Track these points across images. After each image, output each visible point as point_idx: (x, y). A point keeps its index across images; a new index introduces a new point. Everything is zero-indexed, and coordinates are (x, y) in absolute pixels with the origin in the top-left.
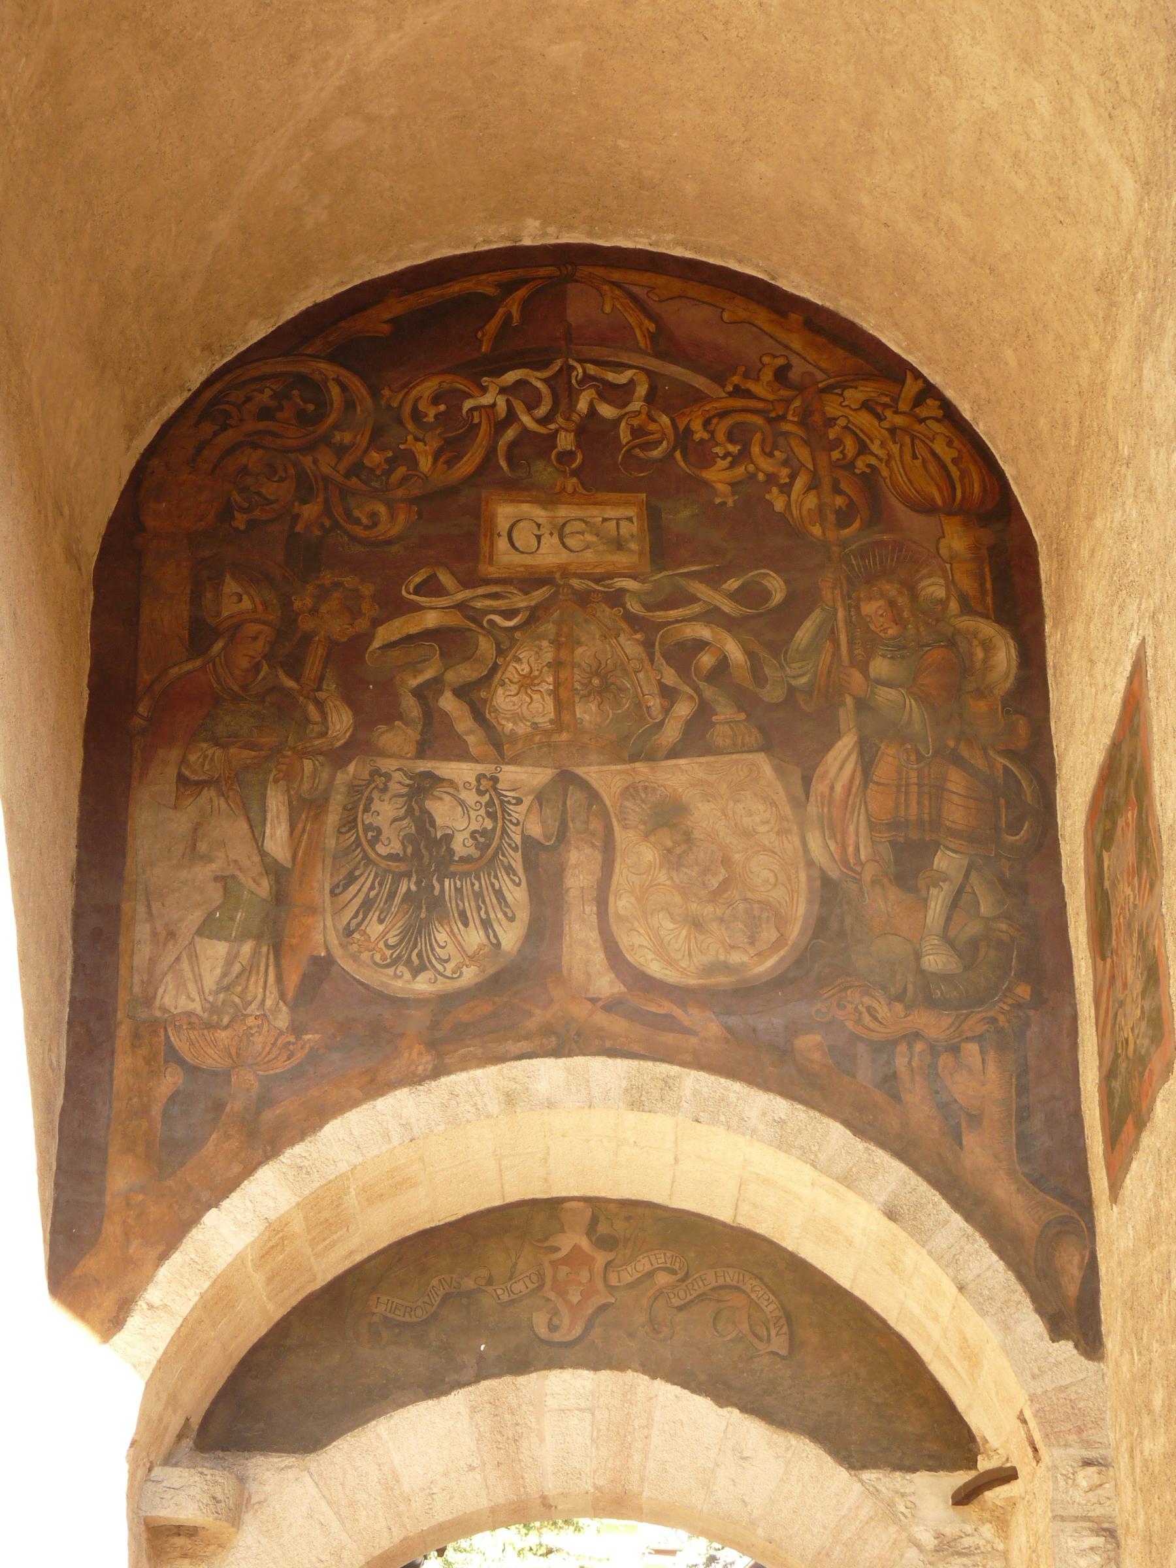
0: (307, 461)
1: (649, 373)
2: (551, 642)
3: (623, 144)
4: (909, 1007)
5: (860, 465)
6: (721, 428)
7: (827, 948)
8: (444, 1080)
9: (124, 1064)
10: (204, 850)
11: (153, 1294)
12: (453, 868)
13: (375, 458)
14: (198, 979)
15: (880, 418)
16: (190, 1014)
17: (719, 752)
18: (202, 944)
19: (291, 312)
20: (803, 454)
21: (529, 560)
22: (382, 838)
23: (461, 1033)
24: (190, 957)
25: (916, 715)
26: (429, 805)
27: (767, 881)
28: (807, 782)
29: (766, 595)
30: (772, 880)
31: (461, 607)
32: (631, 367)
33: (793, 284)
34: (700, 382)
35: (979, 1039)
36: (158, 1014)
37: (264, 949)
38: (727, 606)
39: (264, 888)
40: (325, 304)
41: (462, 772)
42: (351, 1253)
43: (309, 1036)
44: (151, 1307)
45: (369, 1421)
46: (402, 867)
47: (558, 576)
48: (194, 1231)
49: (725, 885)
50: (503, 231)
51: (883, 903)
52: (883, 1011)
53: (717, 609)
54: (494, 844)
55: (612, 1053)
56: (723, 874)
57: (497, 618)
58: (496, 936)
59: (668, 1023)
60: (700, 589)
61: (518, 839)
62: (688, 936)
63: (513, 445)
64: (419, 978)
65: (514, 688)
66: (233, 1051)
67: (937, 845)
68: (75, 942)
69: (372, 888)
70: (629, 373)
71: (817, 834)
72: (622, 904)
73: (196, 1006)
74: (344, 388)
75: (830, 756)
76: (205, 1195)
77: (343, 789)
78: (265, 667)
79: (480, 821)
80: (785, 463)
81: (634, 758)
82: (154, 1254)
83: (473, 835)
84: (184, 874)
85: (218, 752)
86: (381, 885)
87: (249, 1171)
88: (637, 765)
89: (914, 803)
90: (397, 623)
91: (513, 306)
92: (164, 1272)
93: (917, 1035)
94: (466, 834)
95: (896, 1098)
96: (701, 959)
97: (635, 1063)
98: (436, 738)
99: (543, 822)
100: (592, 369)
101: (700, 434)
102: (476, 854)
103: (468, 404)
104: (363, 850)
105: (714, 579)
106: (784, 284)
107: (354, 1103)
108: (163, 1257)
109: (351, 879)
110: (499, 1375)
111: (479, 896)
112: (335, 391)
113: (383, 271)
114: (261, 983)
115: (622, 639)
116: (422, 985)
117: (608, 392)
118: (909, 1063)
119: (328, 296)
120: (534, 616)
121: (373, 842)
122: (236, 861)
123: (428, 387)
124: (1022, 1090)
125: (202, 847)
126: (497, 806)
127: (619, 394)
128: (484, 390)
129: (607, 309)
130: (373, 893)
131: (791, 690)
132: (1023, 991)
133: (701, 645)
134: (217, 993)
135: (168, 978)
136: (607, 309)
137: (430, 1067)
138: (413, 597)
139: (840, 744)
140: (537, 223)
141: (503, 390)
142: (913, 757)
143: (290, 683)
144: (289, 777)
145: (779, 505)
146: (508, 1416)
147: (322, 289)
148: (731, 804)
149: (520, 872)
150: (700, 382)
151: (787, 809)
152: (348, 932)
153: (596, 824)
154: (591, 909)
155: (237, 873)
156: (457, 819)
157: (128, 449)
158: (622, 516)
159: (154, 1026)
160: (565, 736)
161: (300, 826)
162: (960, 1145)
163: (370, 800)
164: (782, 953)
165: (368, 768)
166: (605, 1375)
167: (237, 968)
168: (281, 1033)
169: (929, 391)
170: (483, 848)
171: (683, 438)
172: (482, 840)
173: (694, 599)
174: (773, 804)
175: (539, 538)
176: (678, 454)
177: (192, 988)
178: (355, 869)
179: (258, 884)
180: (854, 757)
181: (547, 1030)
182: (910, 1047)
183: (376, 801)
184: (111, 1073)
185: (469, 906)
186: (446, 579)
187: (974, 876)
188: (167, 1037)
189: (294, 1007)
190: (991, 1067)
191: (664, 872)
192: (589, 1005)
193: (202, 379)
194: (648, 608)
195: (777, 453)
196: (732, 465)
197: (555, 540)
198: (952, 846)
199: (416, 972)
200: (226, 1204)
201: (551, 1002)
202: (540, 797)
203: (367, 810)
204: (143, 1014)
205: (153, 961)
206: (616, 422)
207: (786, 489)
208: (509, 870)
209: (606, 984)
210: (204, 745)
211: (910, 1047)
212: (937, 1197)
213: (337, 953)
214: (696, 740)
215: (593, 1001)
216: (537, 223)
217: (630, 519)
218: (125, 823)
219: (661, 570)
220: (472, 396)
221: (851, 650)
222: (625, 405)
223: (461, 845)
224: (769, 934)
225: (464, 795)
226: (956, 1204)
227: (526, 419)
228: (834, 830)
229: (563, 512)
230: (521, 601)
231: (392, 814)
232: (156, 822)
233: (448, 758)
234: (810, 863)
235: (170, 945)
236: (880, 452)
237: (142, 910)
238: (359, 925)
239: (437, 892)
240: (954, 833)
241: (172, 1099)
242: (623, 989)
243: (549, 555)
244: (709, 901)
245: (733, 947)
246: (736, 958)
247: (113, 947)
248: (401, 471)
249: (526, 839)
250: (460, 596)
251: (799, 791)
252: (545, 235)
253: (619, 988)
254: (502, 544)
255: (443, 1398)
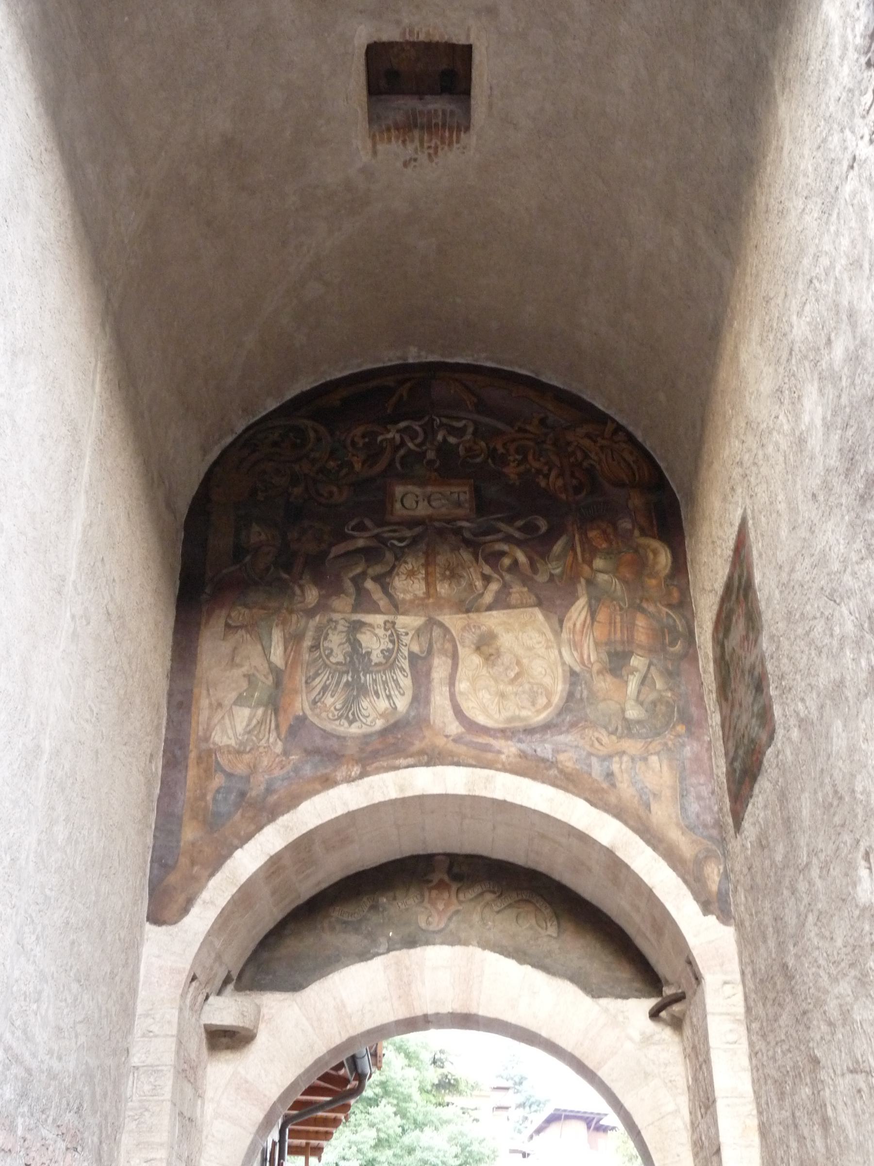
0: (297, 468)
1: (475, 423)
2: (424, 553)
3: (458, 300)
4: (620, 738)
5: (585, 464)
6: (512, 447)
7: (574, 709)
8: (366, 779)
9: (192, 773)
10: (239, 662)
11: (205, 895)
12: (371, 669)
13: (332, 464)
14: (234, 727)
15: (595, 442)
16: (228, 746)
17: (514, 607)
18: (236, 709)
19: (289, 395)
20: (555, 459)
21: (411, 513)
22: (334, 654)
23: (375, 755)
24: (229, 716)
25: (619, 587)
26: (360, 637)
27: (541, 673)
28: (561, 622)
29: (538, 528)
30: (544, 672)
31: (376, 537)
32: (465, 419)
33: (550, 378)
34: (500, 426)
35: (658, 753)
36: (212, 746)
37: (269, 712)
38: (517, 534)
39: (270, 681)
40: (308, 391)
41: (378, 619)
42: (319, 883)
43: (293, 757)
44: (204, 902)
45: (329, 974)
46: (344, 669)
47: (427, 521)
48: (229, 861)
49: (518, 675)
50: (399, 354)
51: (604, 684)
52: (605, 739)
53: (512, 537)
54: (393, 656)
55: (458, 764)
56: (517, 669)
57: (396, 543)
58: (394, 703)
59: (486, 748)
60: (502, 526)
61: (406, 654)
62: (498, 703)
63: (403, 457)
64: (353, 725)
65: (404, 577)
66: (252, 765)
67: (631, 653)
68: (168, 709)
69: (328, 679)
70: (464, 422)
71: (567, 648)
72: (462, 686)
73: (232, 742)
74: (316, 431)
75: (573, 609)
76: (236, 842)
77: (312, 629)
78: (272, 568)
79: (386, 644)
80: (546, 464)
81: (468, 611)
82: (207, 874)
83: (382, 651)
84: (228, 674)
85: (247, 611)
86: (332, 677)
87: (259, 829)
88: (471, 615)
89: (619, 632)
90: (343, 545)
91: (404, 391)
92: (212, 883)
93: (624, 752)
94: (379, 651)
95: (613, 785)
96: (506, 714)
97: (470, 769)
98: (363, 603)
99: (420, 644)
100: (444, 420)
101: (501, 450)
102: (384, 661)
103: (380, 438)
104: (323, 660)
105: (510, 521)
106: (544, 379)
107: (317, 792)
108: (212, 875)
109: (317, 674)
110: (400, 949)
111: (385, 683)
112: (312, 434)
113: (339, 375)
114: (267, 730)
115: (461, 551)
116: (355, 729)
117: (452, 430)
118: (620, 767)
119: (308, 388)
120: (415, 541)
121: (328, 657)
122: (255, 667)
123: (359, 431)
124: (682, 779)
125: (238, 660)
126: (395, 638)
127: (460, 432)
128: (388, 431)
129: (452, 392)
130: (328, 682)
131: (552, 575)
132: (681, 729)
133: (503, 554)
134: (244, 735)
135: (218, 728)
136: (452, 392)
137: (358, 772)
138: (351, 532)
139: (577, 603)
140: (416, 350)
141: (398, 431)
142: (618, 608)
143: (286, 576)
144: (284, 623)
145: (543, 484)
146: (405, 971)
147: (305, 384)
148: (521, 634)
149: (408, 670)
150: (500, 426)
151: (550, 635)
152: (315, 702)
153: (448, 646)
154: (446, 689)
155: (256, 673)
156: (374, 643)
157: (203, 460)
158: (462, 492)
159: (210, 752)
160: (431, 600)
161: (290, 648)
162: (650, 811)
163: (327, 634)
164: (549, 710)
165: (326, 618)
166: (458, 949)
167: (254, 722)
168: (278, 756)
169: (619, 428)
170: (387, 658)
171: (492, 453)
172: (387, 654)
173: (499, 531)
174: (544, 634)
175: (417, 502)
176: (490, 461)
177: (230, 732)
178: (319, 669)
179: (267, 678)
180: (586, 609)
181: (422, 752)
182: (621, 757)
183: (331, 635)
184: (185, 777)
185: (380, 688)
186: (368, 523)
187: (652, 668)
188: (216, 758)
189: (285, 741)
190: (665, 768)
191: (485, 668)
192: (445, 739)
193: (243, 427)
194: (475, 535)
195: (541, 459)
196: (518, 465)
197: (426, 503)
198: (640, 653)
199: (351, 723)
200: (246, 846)
201: (424, 737)
202: (419, 632)
203: (325, 639)
204: (204, 746)
205: (209, 718)
206: (458, 445)
207: (547, 476)
208: (402, 669)
209: (454, 728)
210: (239, 608)
211: (621, 757)
212: (637, 838)
213: (308, 712)
214: (501, 602)
215: (447, 736)
216: (416, 350)
217: (465, 493)
218: (197, 647)
219: (483, 516)
220: (382, 434)
221: (583, 556)
222: (462, 437)
223: (376, 657)
224: (542, 701)
225: (377, 631)
226: (648, 842)
227: (411, 445)
228: (575, 645)
229: (429, 489)
230: (408, 533)
231: (338, 642)
232: (212, 646)
233: (368, 612)
234: (564, 663)
235: (219, 710)
236: (596, 458)
237: (204, 692)
238: (320, 699)
239: (362, 681)
240: (640, 646)
241: (218, 791)
242: (463, 730)
243: (422, 510)
244: (510, 684)
245: (523, 708)
246: (524, 713)
247: (189, 711)
248: (344, 471)
249: (411, 654)
250: (376, 531)
251: (557, 626)
252: (419, 356)
253: (461, 730)
254: (398, 505)
255: (369, 962)
